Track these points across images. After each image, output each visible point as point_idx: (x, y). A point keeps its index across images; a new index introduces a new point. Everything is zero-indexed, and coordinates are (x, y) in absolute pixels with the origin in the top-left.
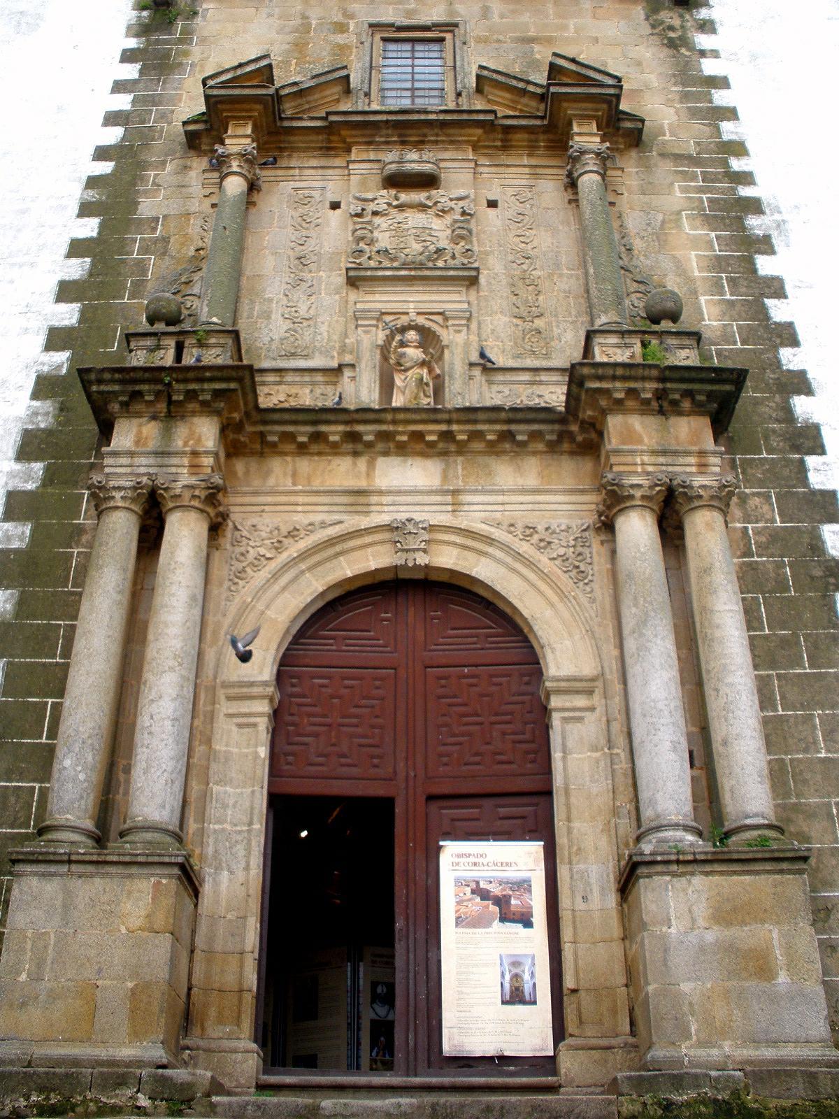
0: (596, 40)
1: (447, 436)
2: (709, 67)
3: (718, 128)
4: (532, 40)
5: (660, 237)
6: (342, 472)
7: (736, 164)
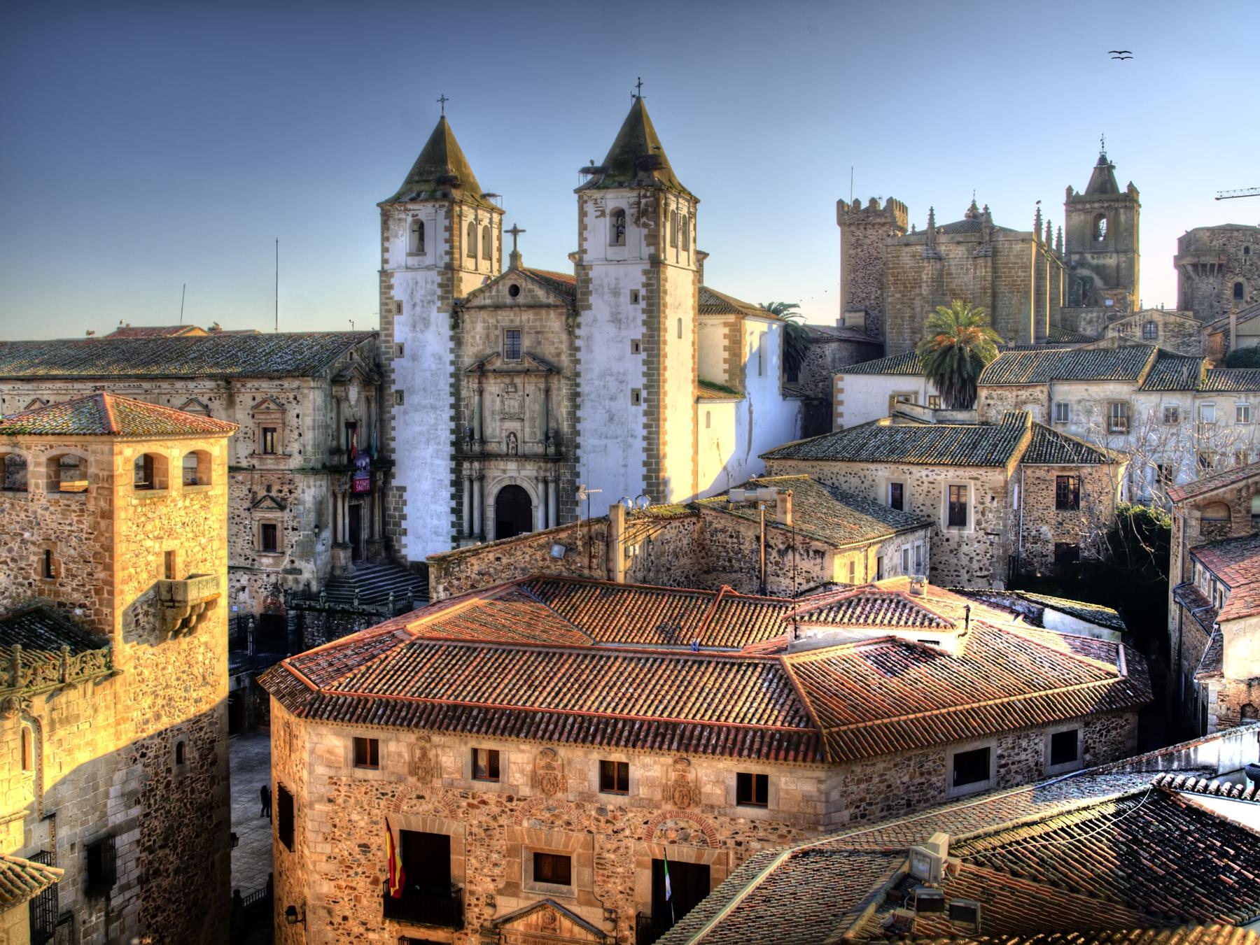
2: (578, 343)
4: (538, 333)
5: (559, 404)
6: (502, 465)
7: (578, 380)
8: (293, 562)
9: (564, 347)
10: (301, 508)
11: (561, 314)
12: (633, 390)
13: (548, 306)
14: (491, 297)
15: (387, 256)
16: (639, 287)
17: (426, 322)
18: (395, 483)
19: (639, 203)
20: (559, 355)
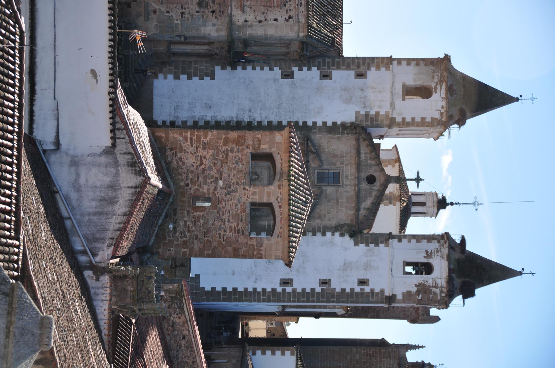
2: (329, 234)
3: (310, 232)
8: (155, 12)
9: (326, 222)
10: (201, 22)
11: (352, 220)
12: (292, 280)
13: (358, 210)
14: (366, 159)
15: (404, 63)
16: (372, 285)
17: (348, 101)
18: (218, 69)
19: (436, 287)
20: (320, 217)
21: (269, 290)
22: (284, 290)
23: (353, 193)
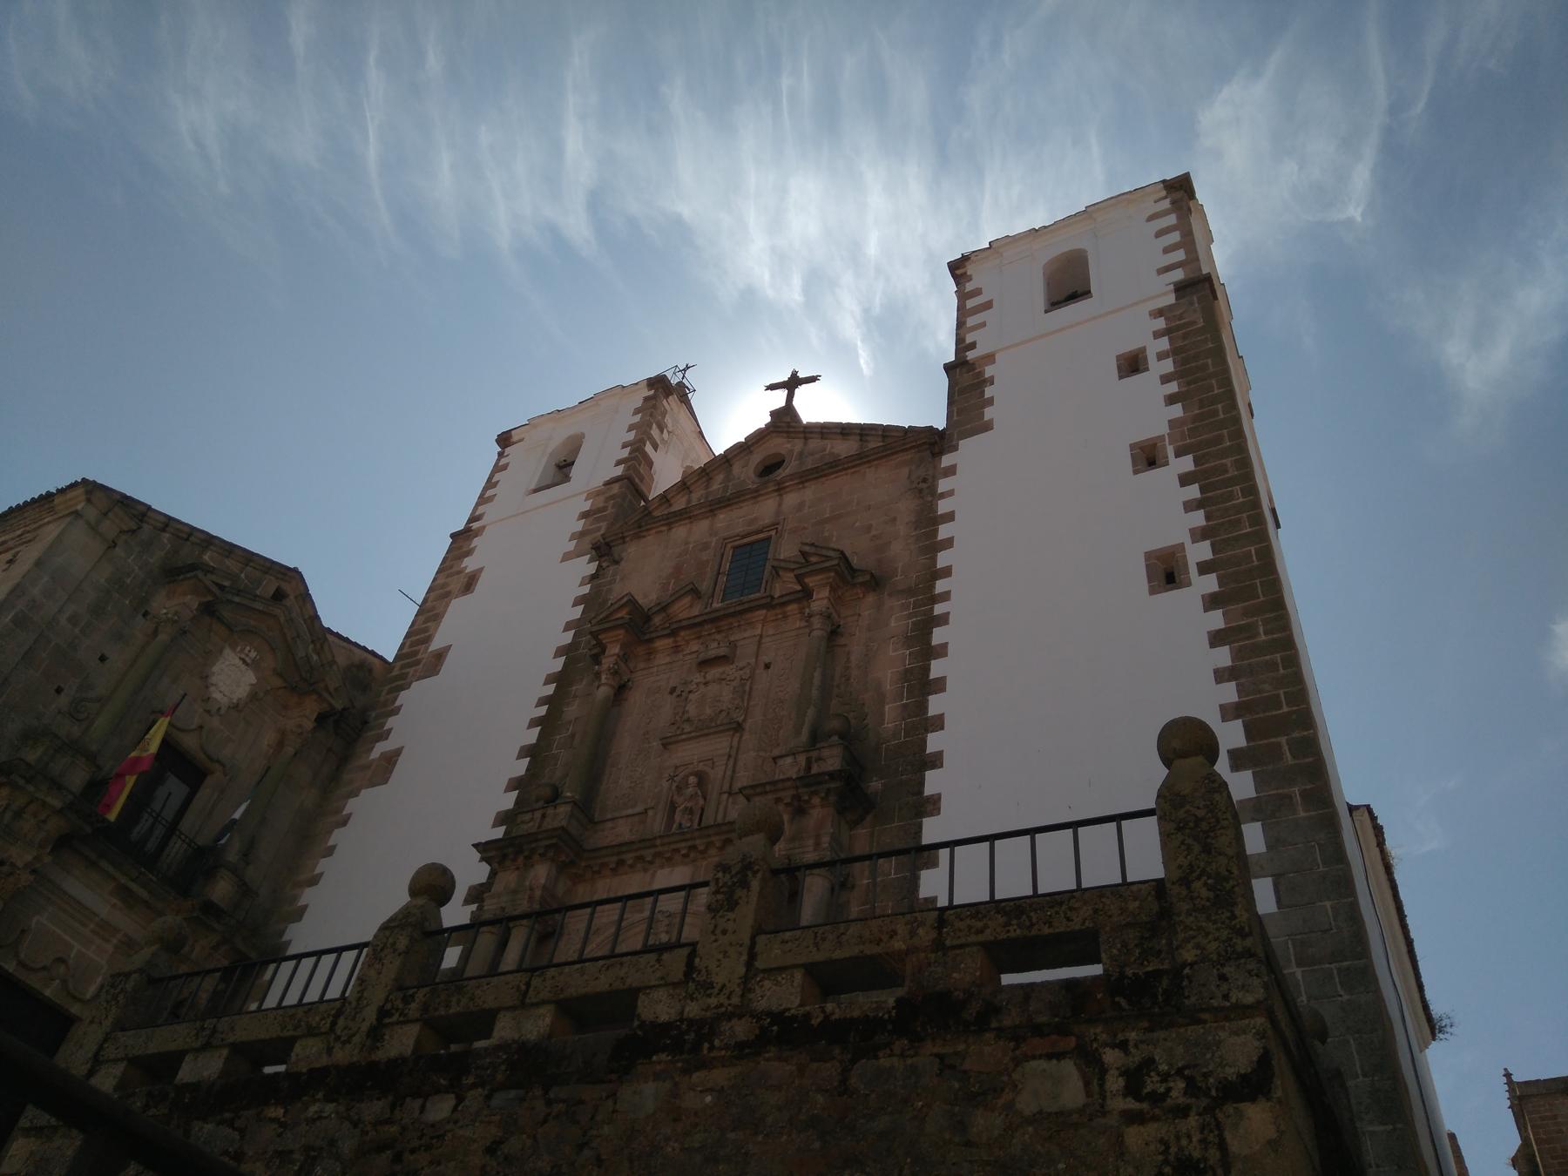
0: (869, 508)
1: (694, 847)
2: (943, 507)
21: (1216, 620)
22: (1204, 568)
23: (810, 492)
